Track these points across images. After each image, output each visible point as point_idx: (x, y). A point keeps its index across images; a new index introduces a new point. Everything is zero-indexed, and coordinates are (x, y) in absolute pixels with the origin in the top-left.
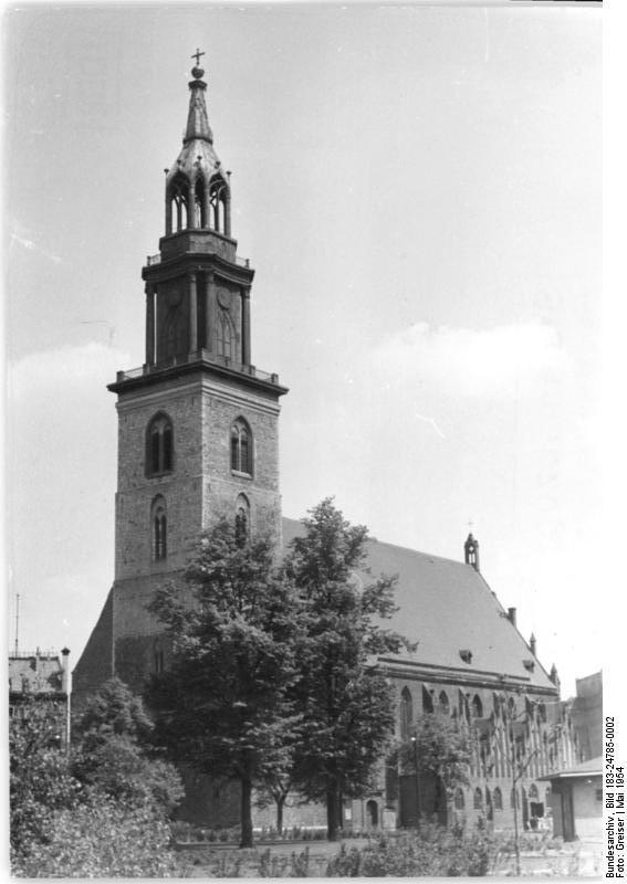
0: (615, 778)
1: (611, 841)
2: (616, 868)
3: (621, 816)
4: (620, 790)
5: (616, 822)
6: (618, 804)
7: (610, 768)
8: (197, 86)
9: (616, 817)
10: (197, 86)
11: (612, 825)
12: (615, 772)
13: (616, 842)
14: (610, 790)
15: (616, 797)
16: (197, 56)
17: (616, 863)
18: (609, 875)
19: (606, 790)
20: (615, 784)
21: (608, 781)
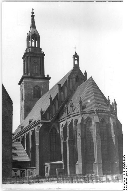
0: (125, 168)
1: (125, 182)
2: (126, 188)
3: (127, 176)
4: (126, 171)
5: (126, 178)
6: (126, 174)
7: (124, 166)
8: (33, 16)
9: (126, 177)
10: (33, 16)
11: (125, 178)
12: (125, 167)
13: (126, 182)
14: (124, 171)
15: (126, 172)
17: (126, 186)
18: (124, 189)
19: (123, 171)
20: (125, 169)
21: (124, 169)
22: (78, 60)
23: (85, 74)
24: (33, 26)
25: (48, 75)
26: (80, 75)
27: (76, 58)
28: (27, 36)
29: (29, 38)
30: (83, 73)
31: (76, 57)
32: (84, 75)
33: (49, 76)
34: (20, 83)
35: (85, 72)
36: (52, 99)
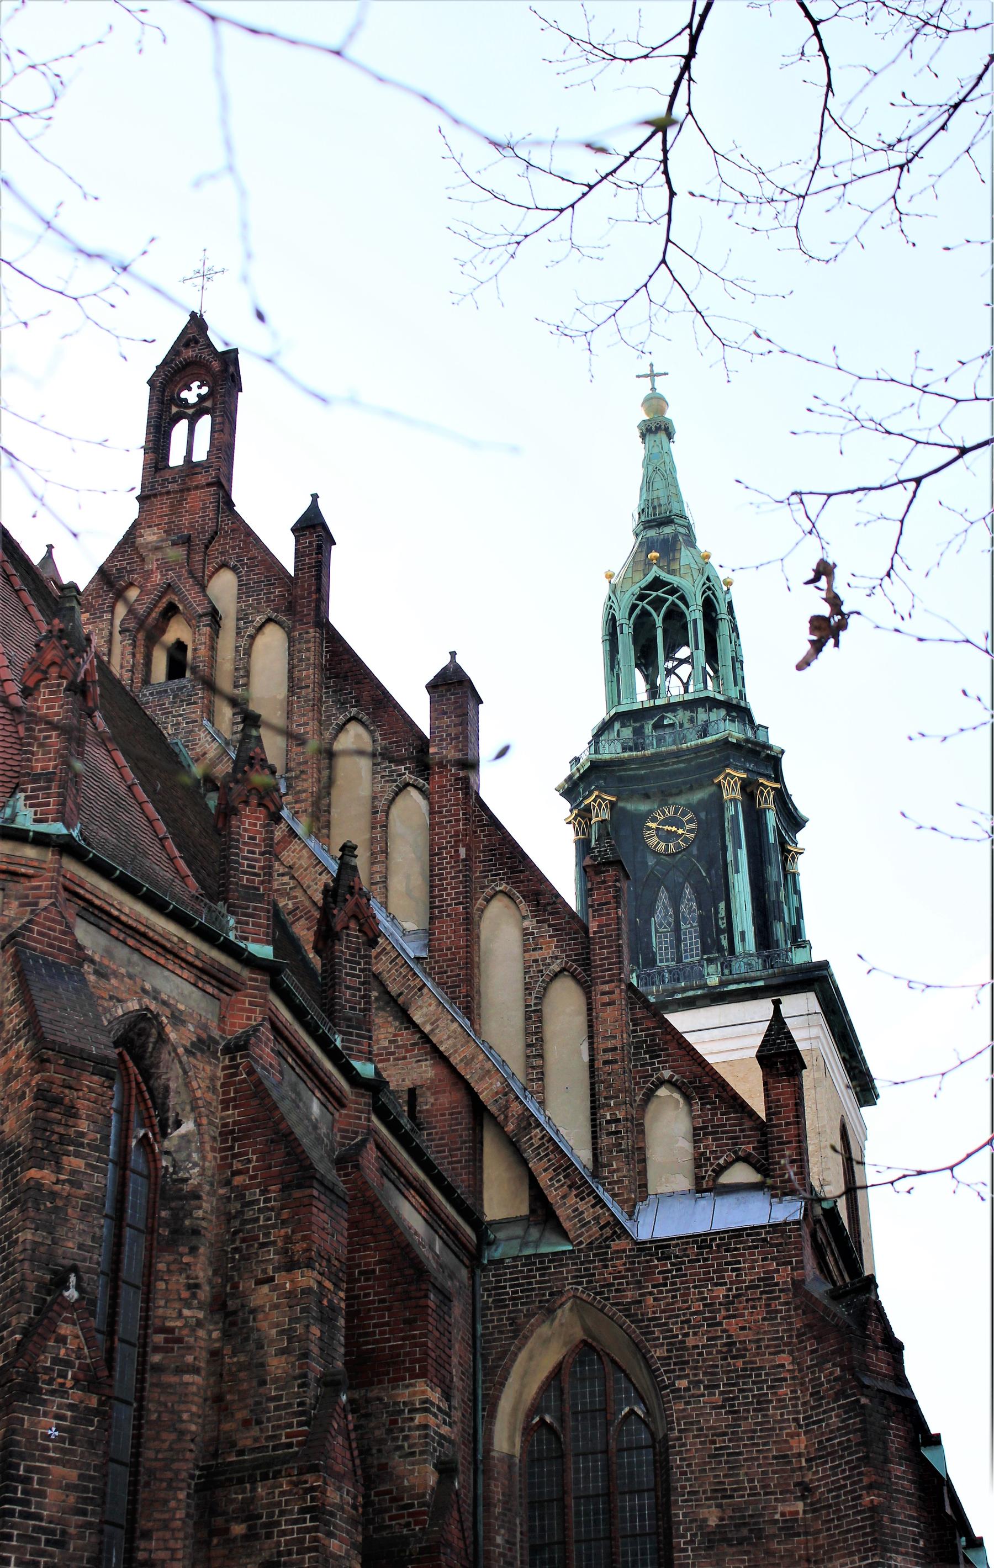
16: (652, 375)
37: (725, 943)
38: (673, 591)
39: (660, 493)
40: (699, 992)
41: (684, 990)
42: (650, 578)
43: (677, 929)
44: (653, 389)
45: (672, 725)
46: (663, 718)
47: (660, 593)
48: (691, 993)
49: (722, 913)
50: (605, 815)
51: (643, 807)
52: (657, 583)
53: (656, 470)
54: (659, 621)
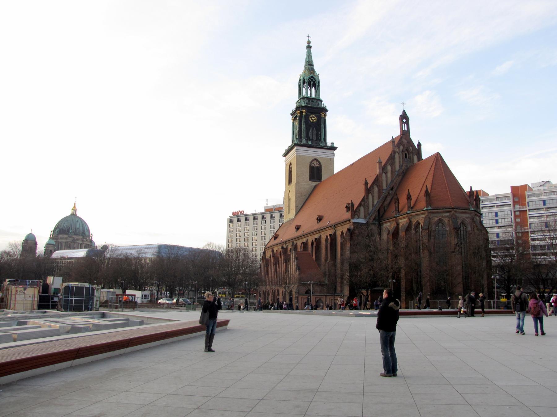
8: (309, 47)
10: (309, 47)
22: (407, 123)
23: (417, 146)
24: (309, 64)
25: (333, 143)
26: (411, 148)
27: (404, 120)
28: (300, 80)
29: (302, 82)
30: (416, 144)
31: (404, 118)
32: (417, 147)
33: (335, 146)
34: (285, 155)
35: (419, 142)
36: (369, 186)
37: (320, 139)
38: (314, 79)
39: (310, 59)
40: (320, 147)
41: (318, 146)
42: (311, 76)
43: (313, 134)
44: (309, 39)
45: (314, 102)
46: (312, 100)
47: (312, 79)
48: (319, 147)
49: (320, 134)
50: (305, 114)
51: (309, 114)
52: (312, 77)
53: (310, 55)
54: (312, 83)
